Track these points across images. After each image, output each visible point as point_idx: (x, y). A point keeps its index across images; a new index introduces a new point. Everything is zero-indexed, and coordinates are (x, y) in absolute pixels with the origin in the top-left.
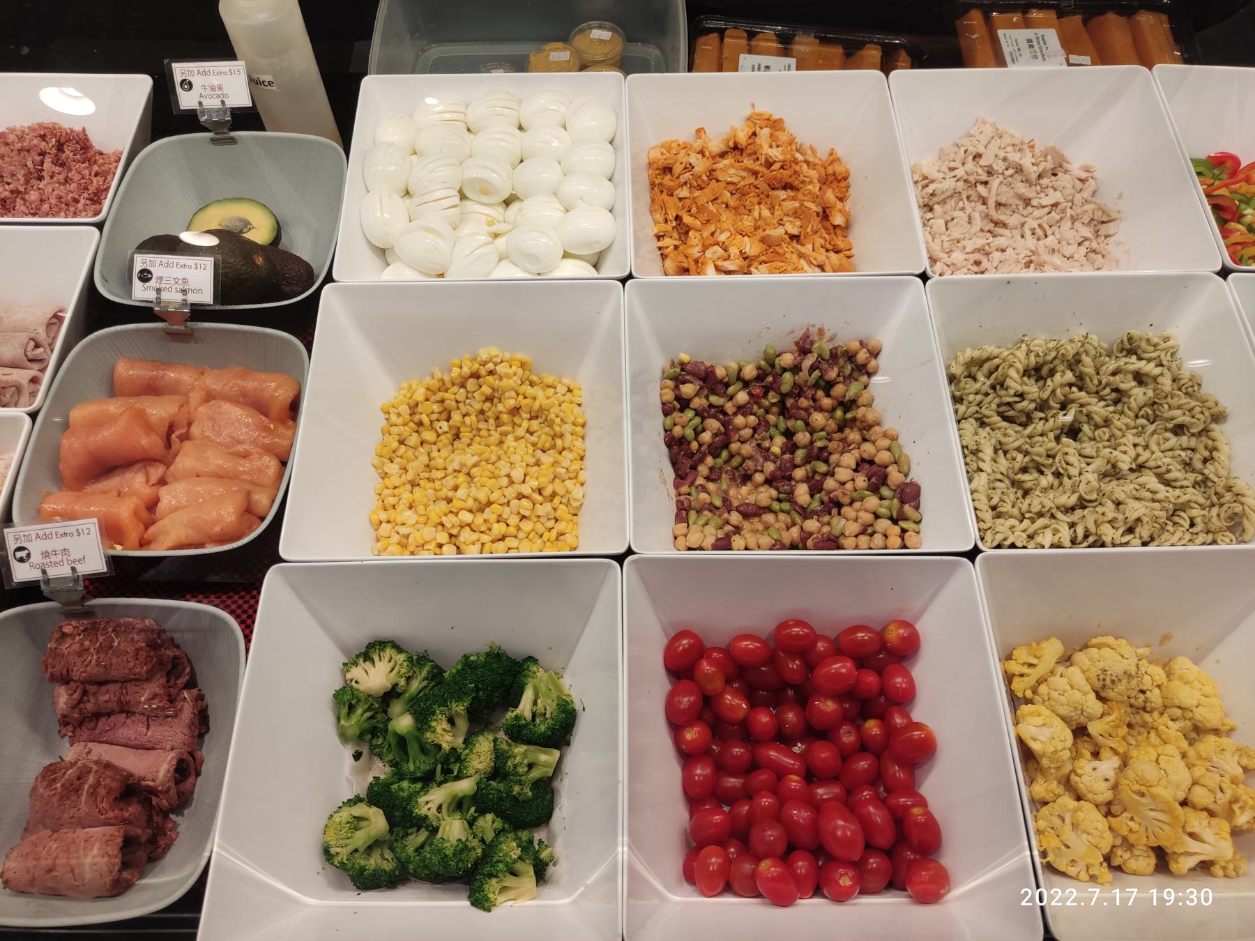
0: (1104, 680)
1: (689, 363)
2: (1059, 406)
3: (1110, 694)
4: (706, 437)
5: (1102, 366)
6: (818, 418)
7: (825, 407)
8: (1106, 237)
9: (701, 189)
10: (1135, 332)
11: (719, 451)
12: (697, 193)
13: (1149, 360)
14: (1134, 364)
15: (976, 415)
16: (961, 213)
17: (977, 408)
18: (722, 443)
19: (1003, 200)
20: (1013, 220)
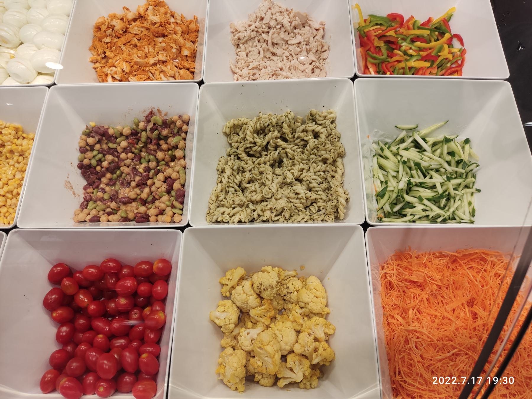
0: (260, 289)
1: (95, 127)
2: (274, 149)
3: (264, 295)
4: (105, 164)
5: (297, 128)
6: (160, 155)
7: (164, 149)
8: (324, 60)
9: (118, 38)
10: (314, 111)
11: (115, 170)
12: (116, 40)
13: (320, 125)
14: (312, 126)
15: (234, 153)
16: (255, 49)
17: (236, 150)
18: (114, 168)
19: (275, 41)
20: (278, 51)
